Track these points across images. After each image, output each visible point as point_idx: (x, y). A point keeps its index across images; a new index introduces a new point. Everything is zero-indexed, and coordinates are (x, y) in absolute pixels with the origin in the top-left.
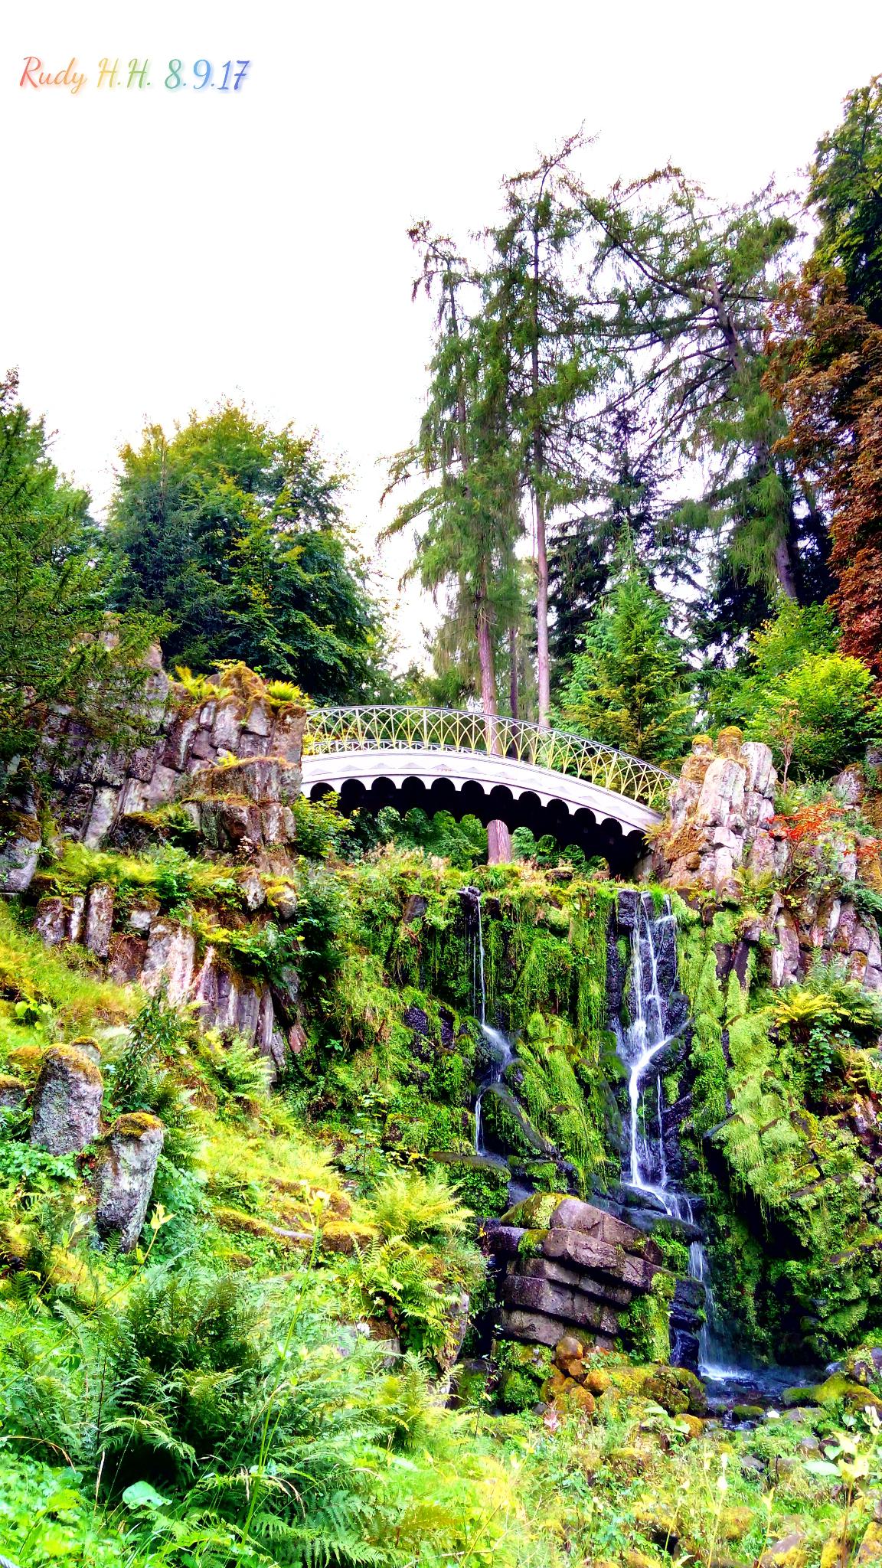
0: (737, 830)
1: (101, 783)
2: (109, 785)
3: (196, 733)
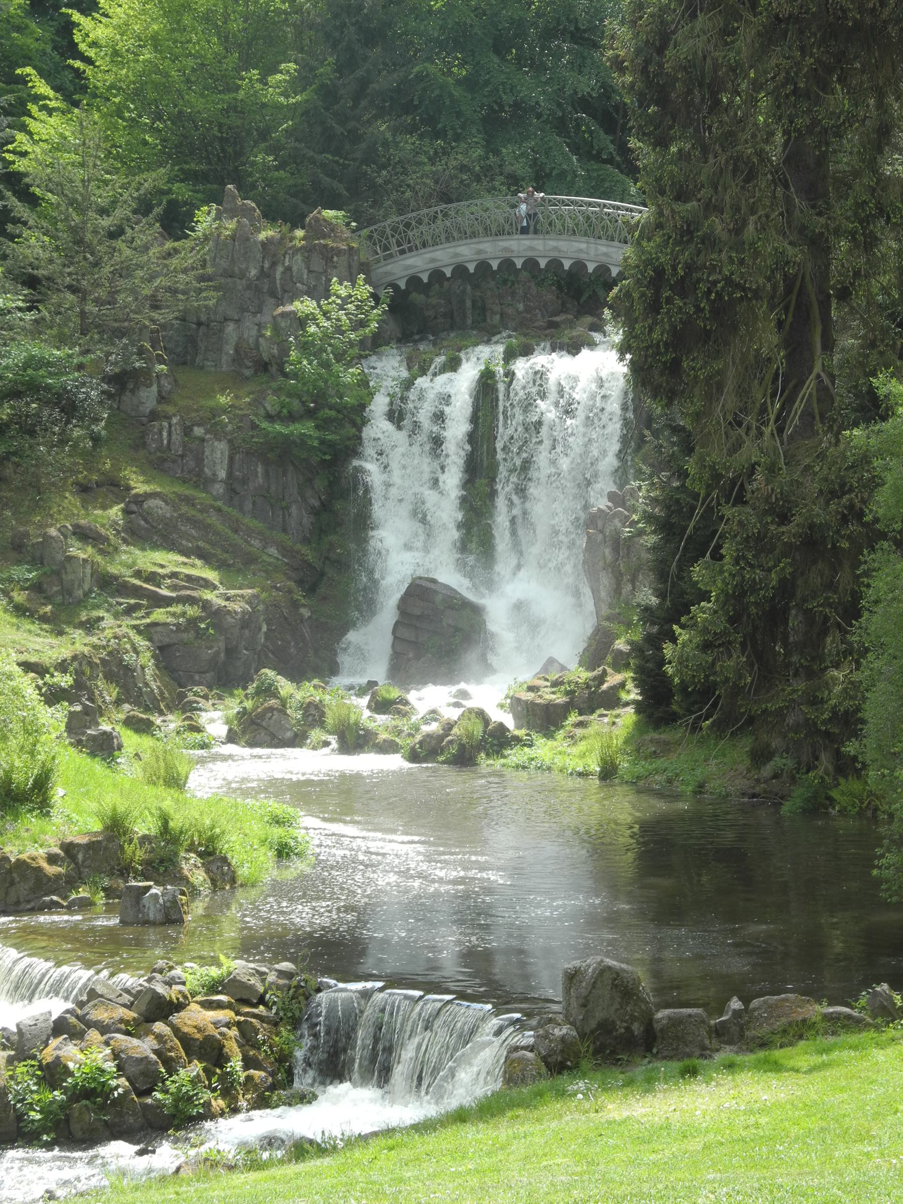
3: (283, 273)
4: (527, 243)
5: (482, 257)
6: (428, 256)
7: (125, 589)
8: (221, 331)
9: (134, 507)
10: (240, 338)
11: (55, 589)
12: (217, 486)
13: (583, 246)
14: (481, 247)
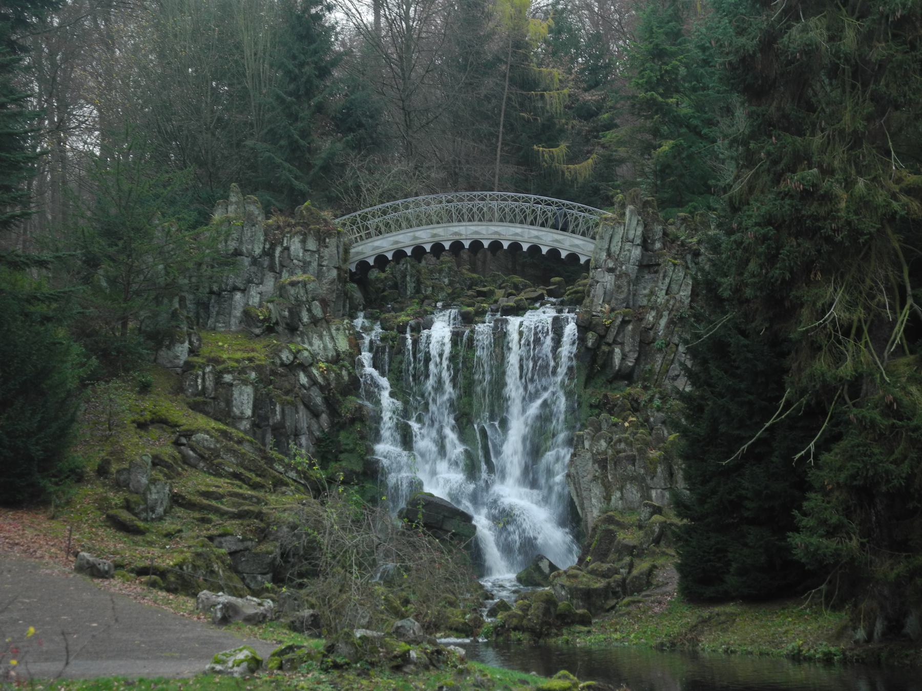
0: (610, 270)
1: (235, 289)
2: (239, 289)
3: (282, 252)
4: (474, 228)
5: (436, 239)
6: (391, 239)
7: (190, 506)
8: (231, 298)
9: (184, 440)
10: (247, 304)
11: (141, 507)
12: (244, 422)
13: (519, 231)
14: (435, 231)
